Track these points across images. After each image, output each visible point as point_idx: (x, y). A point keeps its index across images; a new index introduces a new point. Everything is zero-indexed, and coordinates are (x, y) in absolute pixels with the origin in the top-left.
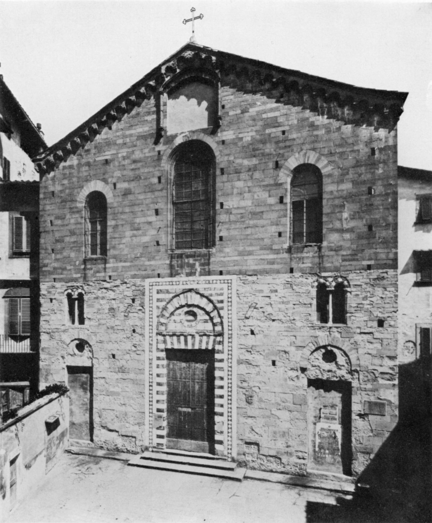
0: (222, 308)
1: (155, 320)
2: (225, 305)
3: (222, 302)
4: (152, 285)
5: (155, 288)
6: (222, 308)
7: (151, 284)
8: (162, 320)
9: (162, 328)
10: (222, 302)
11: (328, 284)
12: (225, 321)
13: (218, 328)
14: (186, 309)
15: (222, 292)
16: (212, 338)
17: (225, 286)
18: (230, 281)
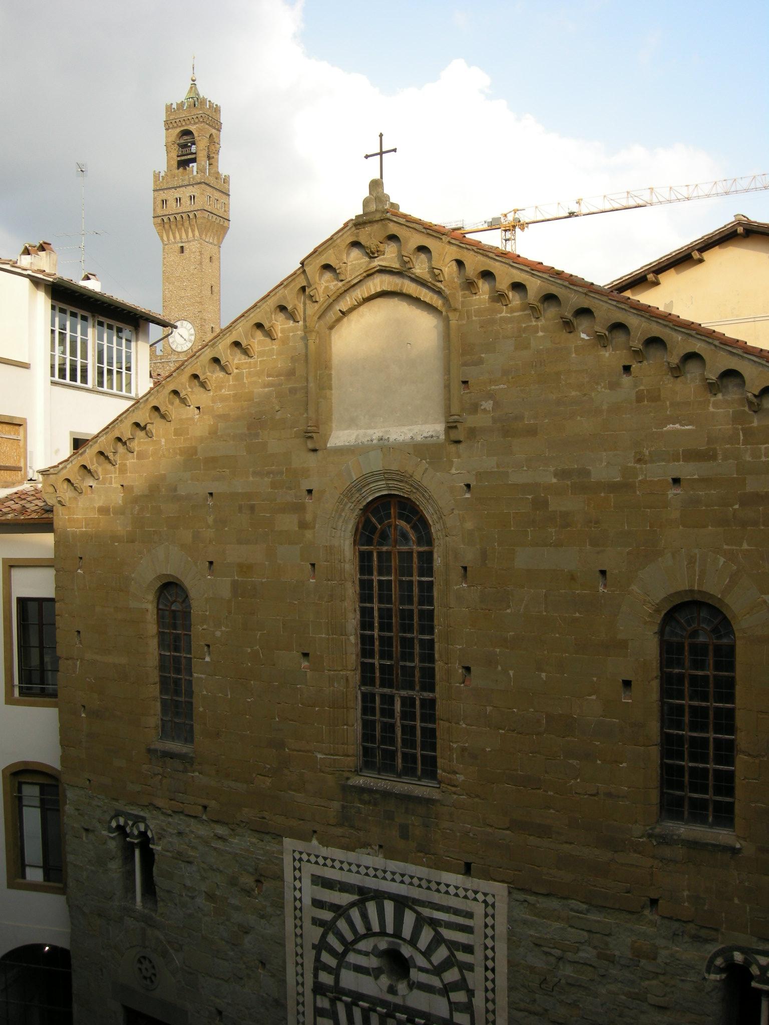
0: (471, 967)
1: (310, 955)
3: (468, 949)
5: (309, 870)
6: (471, 967)
7: (297, 856)
10: (468, 949)
11: (755, 970)
14: (383, 944)
17: (478, 909)
18: (490, 900)
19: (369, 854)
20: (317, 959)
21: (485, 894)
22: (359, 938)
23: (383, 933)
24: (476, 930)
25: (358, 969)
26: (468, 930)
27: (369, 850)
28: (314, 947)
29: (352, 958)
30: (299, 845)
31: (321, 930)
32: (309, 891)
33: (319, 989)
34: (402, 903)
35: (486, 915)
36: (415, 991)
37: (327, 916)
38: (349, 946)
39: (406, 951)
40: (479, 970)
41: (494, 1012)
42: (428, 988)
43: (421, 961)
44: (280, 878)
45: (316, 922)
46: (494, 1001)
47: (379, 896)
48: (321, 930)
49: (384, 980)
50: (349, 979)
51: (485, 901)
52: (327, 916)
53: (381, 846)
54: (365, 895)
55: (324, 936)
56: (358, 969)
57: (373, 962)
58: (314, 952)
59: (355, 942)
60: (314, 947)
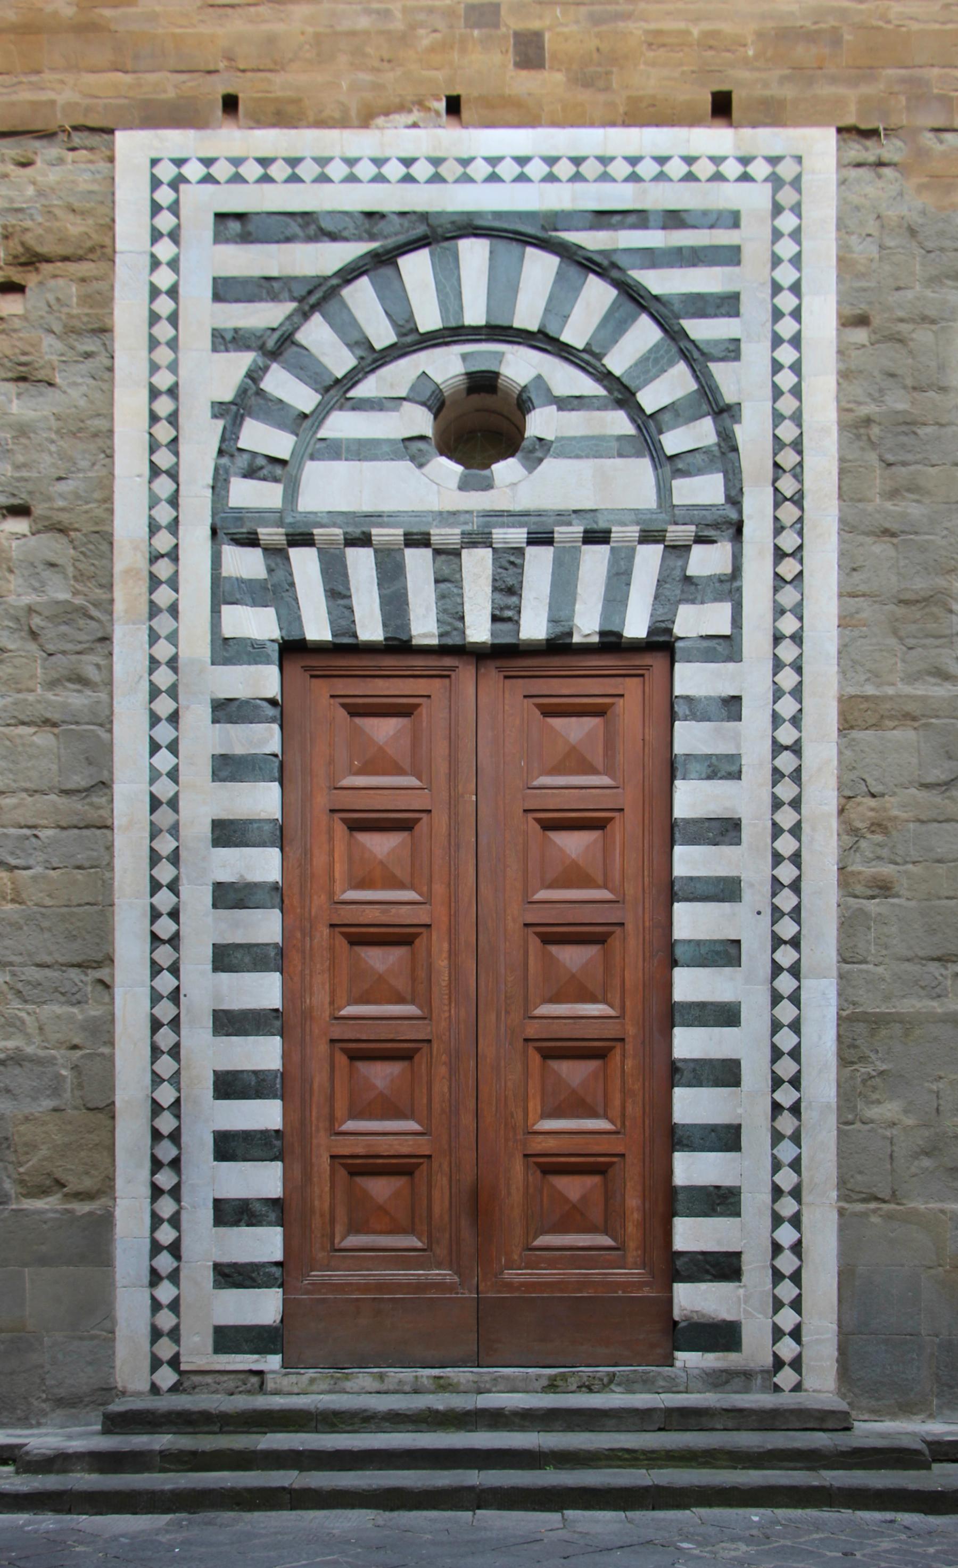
0: (732, 350)
2: (749, 326)
3: (728, 305)
4: (177, 183)
6: (732, 350)
7: (166, 172)
8: (258, 437)
9: (247, 494)
10: (728, 305)
12: (753, 434)
13: (705, 490)
14: (446, 366)
15: (723, 237)
16: (649, 559)
17: (753, 199)
18: (786, 170)
19: (415, 125)
20: (227, 448)
21: (774, 161)
22: (375, 359)
23: (454, 334)
24: (746, 255)
25: (363, 450)
26: (731, 256)
27: (415, 116)
28: (219, 409)
29: (342, 425)
30: (175, 141)
31: (245, 360)
32: (208, 259)
33: (232, 530)
34: (513, 234)
35: (777, 209)
36: (550, 465)
37: (267, 315)
38: (337, 391)
39: (519, 366)
40: (756, 354)
41: (798, 446)
42: (591, 447)
43: (568, 380)
44: (101, 251)
45: (224, 340)
46: (797, 418)
47: (438, 234)
48: (245, 360)
49: (448, 469)
50: (328, 490)
51: (776, 181)
52: (267, 315)
53: (454, 106)
54: (390, 242)
55: (255, 375)
56: (363, 450)
57: (420, 421)
58: (220, 424)
59: (354, 377)
60: (219, 409)
